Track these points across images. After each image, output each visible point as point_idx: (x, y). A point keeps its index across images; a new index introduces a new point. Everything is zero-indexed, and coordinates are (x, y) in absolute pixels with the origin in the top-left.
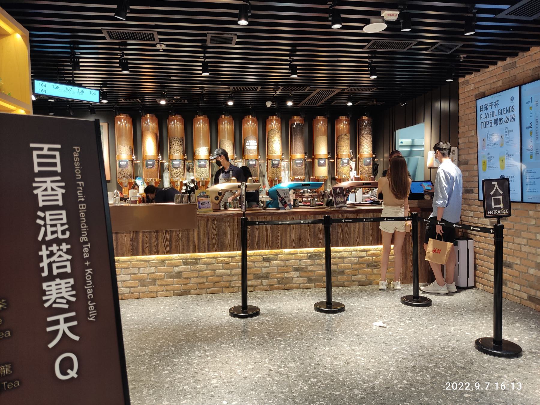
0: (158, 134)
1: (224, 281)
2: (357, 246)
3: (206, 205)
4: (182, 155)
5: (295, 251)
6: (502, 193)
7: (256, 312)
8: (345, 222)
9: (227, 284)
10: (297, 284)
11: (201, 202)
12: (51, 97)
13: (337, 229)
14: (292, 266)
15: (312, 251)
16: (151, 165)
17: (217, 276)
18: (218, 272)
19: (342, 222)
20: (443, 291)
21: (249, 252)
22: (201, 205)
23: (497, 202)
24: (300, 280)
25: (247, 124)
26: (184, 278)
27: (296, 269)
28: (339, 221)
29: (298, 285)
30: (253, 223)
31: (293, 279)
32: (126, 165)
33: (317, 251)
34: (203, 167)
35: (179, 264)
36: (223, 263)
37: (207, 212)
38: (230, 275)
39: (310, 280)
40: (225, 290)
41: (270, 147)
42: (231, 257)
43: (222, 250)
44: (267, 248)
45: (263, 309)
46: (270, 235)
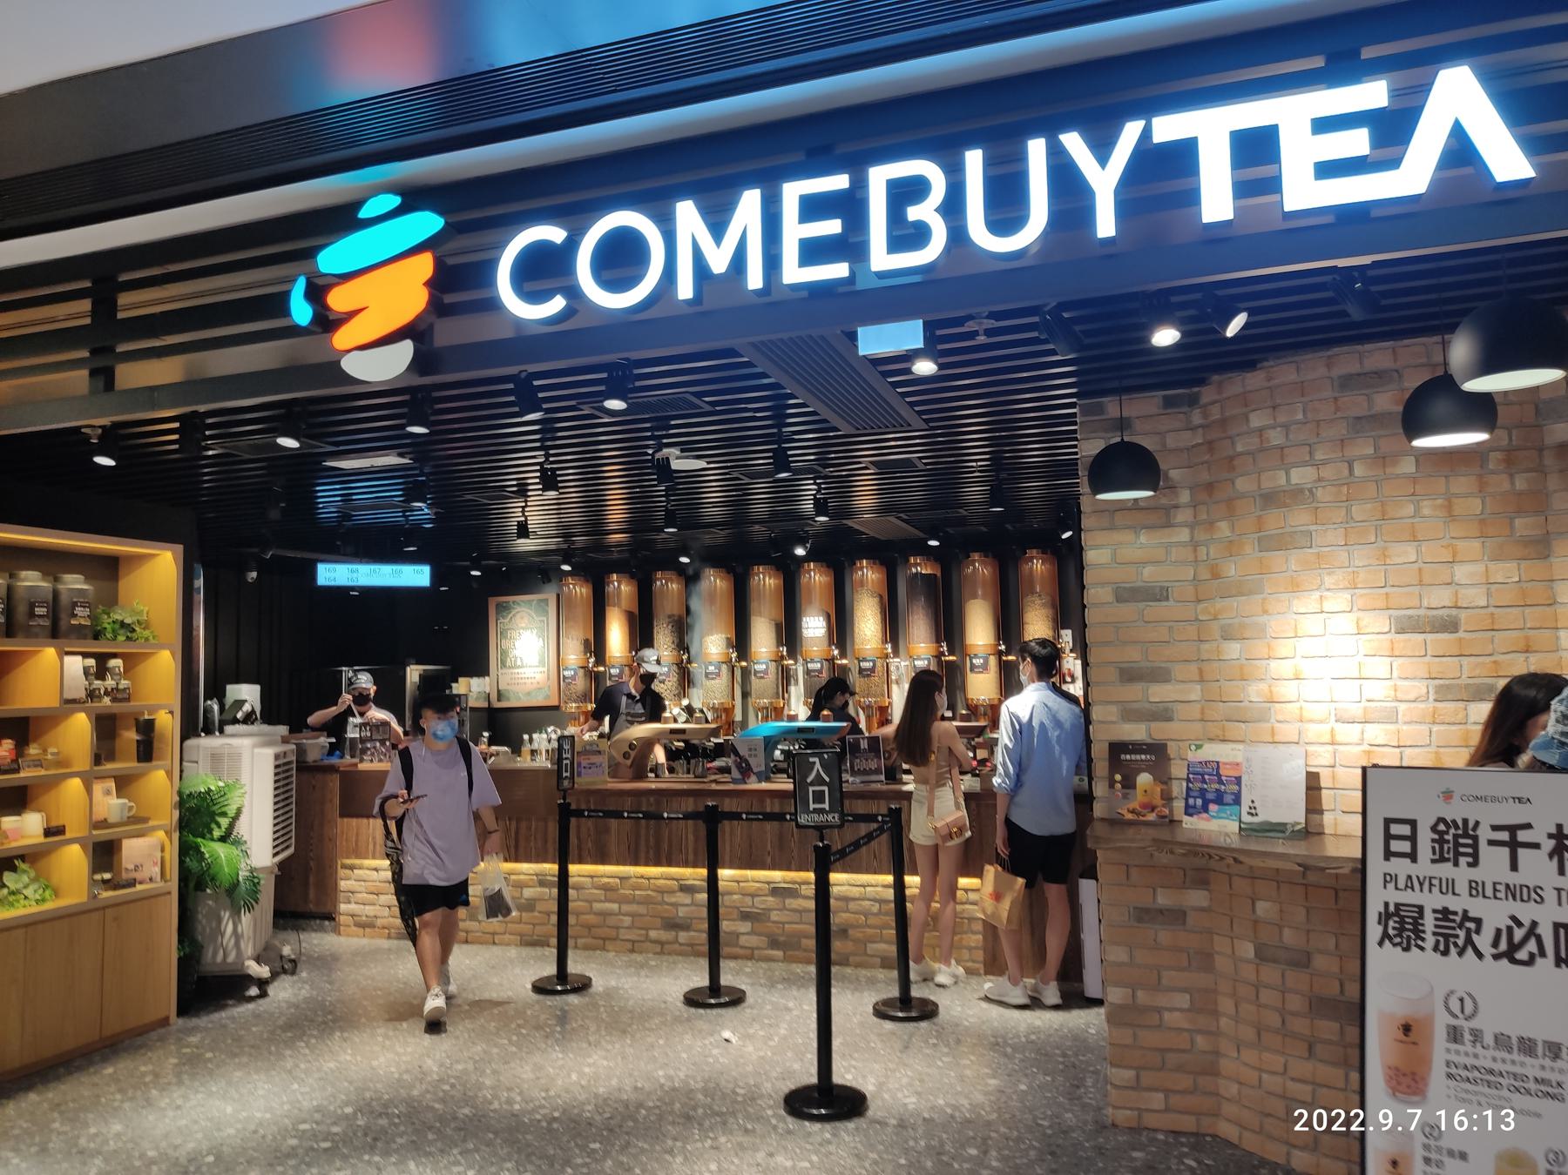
0: (636, 611)
1: (609, 927)
2: (875, 873)
3: (594, 769)
4: (675, 653)
5: (741, 876)
6: (827, 779)
7: (583, 986)
8: (628, 817)
9: (613, 933)
10: (746, 948)
11: (584, 763)
12: (353, 588)
13: (731, 834)
14: (738, 908)
15: (779, 879)
16: (615, 676)
17: (595, 914)
18: (597, 906)
19: (742, 819)
20: (1015, 997)
21: (573, 868)
22: (583, 770)
23: (819, 797)
24: (753, 941)
25: (908, 561)
26: (540, 912)
27: (745, 916)
28: (735, 816)
29: (749, 952)
30: (579, 813)
31: (738, 937)
32: (573, 678)
33: (788, 879)
34: (713, 679)
35: (531, 884)
36: (607, 888)
37: (594, 783)
38: (616, 915)
39: (774, 943)
40: (609, 945)
41: (856, 630)
42: (621, 878)
43: (603, 862)
44: (686, 864)
45: (598, 984)
46: (691, 837)
